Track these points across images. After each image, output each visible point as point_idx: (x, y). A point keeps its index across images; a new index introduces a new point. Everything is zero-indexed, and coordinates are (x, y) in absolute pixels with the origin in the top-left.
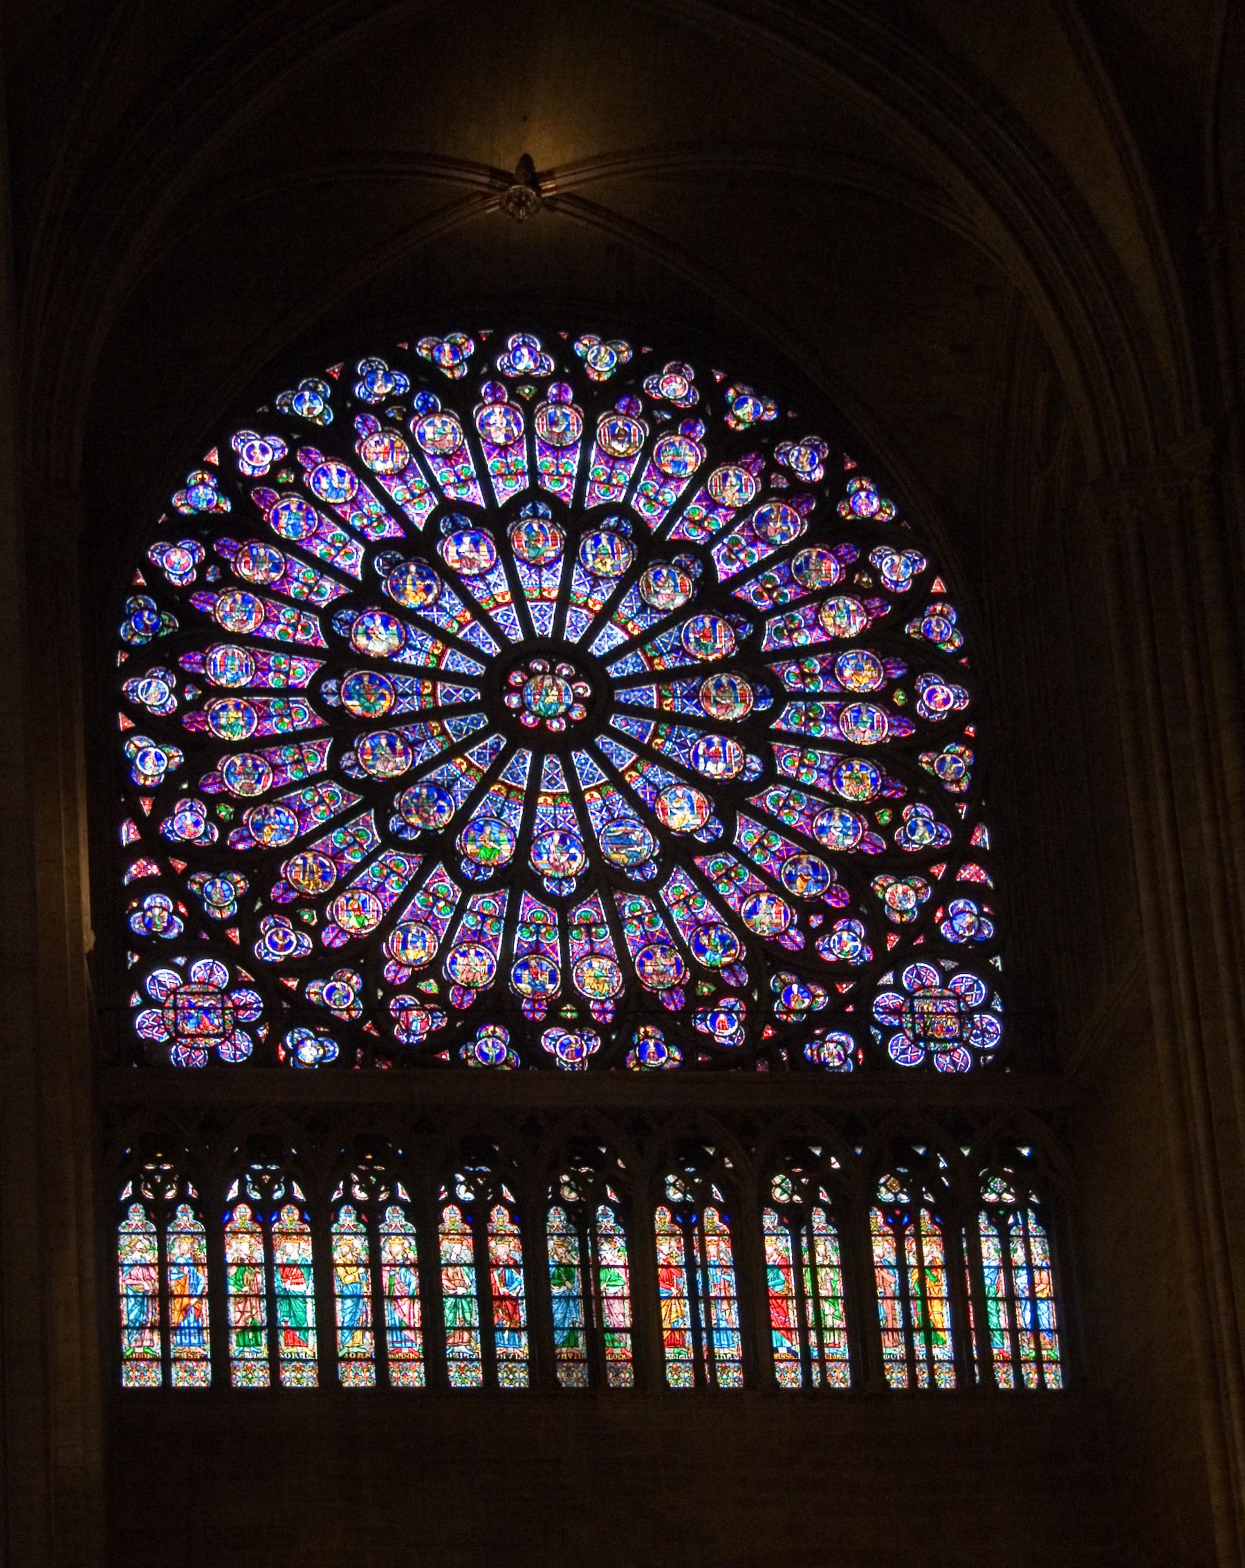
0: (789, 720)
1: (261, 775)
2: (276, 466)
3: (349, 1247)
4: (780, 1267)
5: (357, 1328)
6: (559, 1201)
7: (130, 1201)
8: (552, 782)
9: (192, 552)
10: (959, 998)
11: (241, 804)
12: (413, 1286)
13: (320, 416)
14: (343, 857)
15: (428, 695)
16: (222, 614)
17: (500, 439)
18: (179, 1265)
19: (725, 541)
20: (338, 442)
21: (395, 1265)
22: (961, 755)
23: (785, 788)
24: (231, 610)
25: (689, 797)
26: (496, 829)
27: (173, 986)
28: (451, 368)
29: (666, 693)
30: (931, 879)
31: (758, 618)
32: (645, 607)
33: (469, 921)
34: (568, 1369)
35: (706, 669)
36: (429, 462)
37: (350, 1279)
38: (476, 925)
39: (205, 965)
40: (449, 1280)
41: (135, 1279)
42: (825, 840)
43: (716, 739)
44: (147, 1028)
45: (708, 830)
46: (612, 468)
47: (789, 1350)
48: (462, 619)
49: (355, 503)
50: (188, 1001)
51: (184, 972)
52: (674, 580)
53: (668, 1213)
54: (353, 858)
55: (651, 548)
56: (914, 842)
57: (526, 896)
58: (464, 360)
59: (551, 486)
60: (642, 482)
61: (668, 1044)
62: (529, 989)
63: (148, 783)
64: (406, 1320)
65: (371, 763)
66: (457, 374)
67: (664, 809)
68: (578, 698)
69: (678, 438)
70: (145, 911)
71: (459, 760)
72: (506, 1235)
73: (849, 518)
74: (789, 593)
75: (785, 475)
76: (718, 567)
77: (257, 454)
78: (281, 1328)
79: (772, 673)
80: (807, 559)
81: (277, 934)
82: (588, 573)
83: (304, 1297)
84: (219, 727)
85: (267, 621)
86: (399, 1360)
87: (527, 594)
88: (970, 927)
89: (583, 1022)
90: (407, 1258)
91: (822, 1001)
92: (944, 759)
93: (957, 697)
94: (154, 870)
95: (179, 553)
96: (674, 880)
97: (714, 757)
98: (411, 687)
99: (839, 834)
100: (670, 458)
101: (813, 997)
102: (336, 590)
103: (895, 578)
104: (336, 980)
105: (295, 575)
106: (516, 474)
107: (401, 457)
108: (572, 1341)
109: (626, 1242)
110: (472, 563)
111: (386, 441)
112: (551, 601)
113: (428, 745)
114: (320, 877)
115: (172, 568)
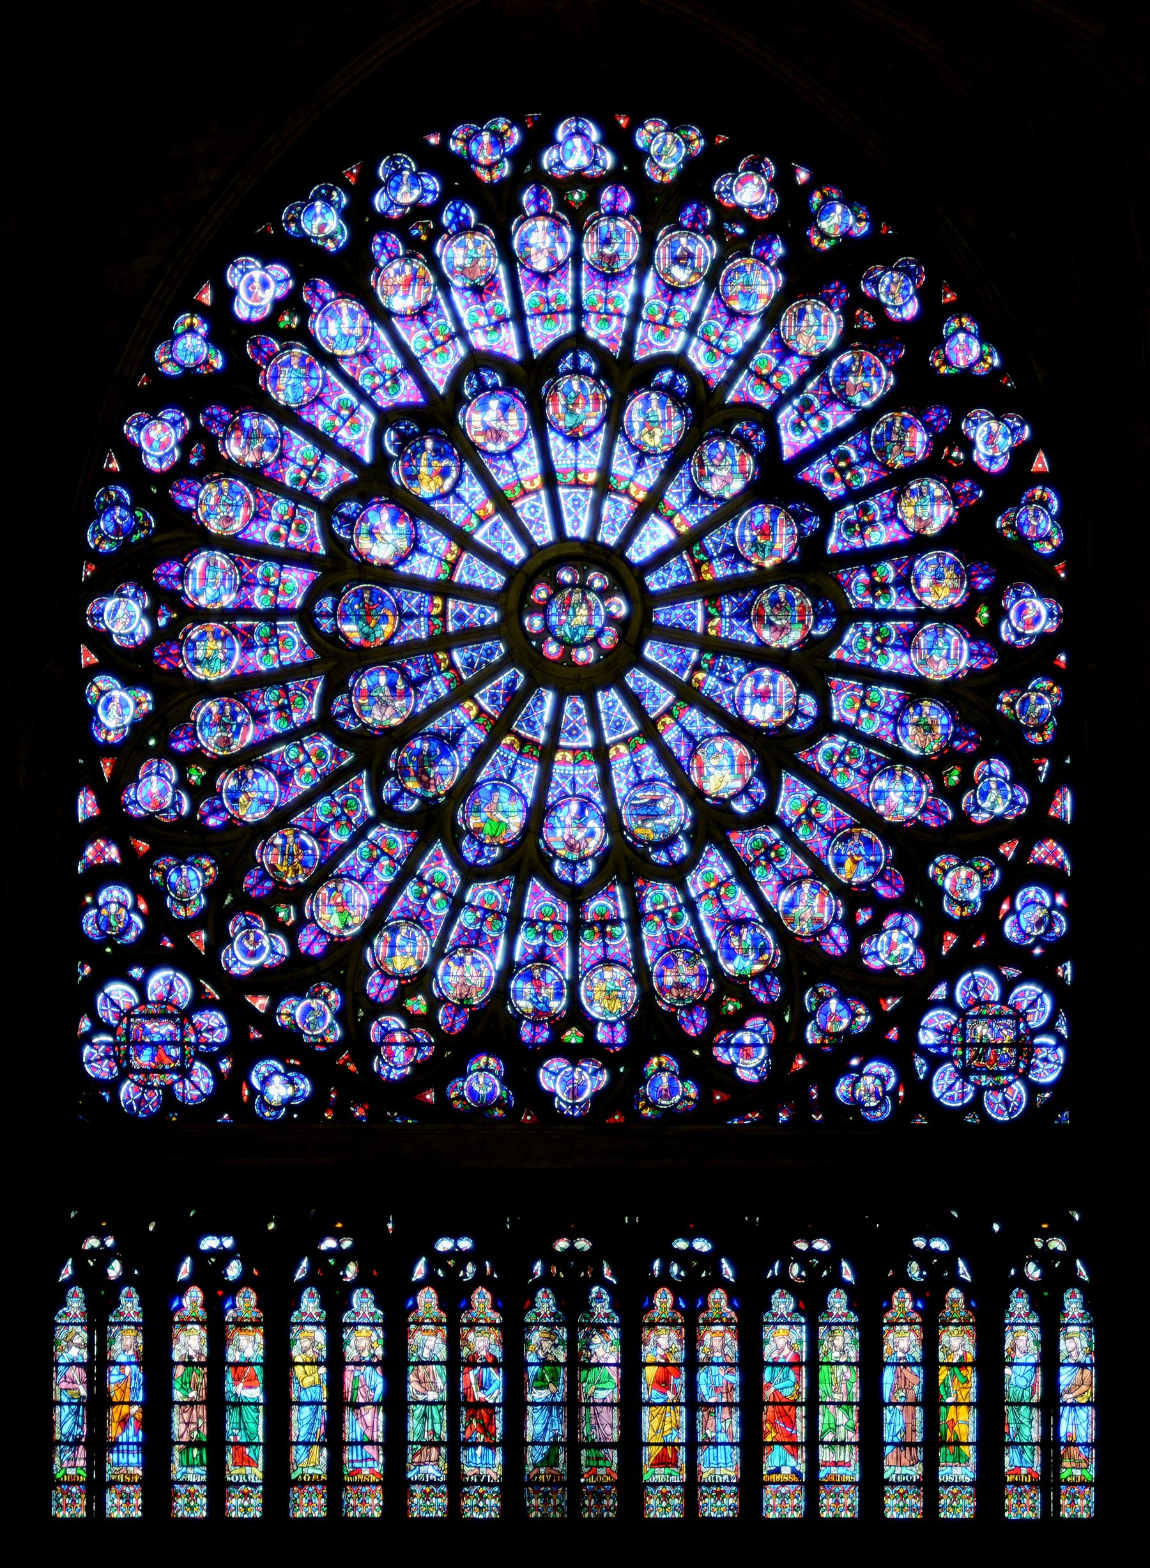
0: (854, 645)
1: (239, 726)
2: (279, 306)
3: (309, 1341)
4: (790, 1365)
5: (313, 1444)
6: (546, 1281)
7: (69, 1283)
8: (574, 733)
9: (174, 424)
10: (1019, 1016)
11: (216, 766)
12: (380, 1389)
13: (331, 237)
14: (327, 835)
15: (437, 616)
16: (205, 508)
17: (542, 265)
18: (120, 1364)
19: (796, 402)
20: (351, 273)
21: (358, 1364)
22: (1048, 693)
23: (841, 739)
24: (217, 504)
25: (730, 752)
26: (504, 795)
27: (127, 1006)
28: (490, 167)
29: (712, 611)
30: (1000, 861)
31: (827, 509)
32: (697, 494)
33: (466, 918)
34: (545, 1494)
35: (761, 580)
36: (455, 296)
37: (309, 1381)
38: (475, 923)
39: (165, 978)
40: (420, 1383)
41: (69, 1384)
42: (882, 809)
43: (767, 672)
44: (96, 1061)
45: (749, 795)
46: (671, 303)
47: (793, 1468)
48: (481, 513)
49: (366, 356)
50: (143, 1025)
51: (140, 986)
52: (733, 457)
53: (669, 1296)
54: (338, 836)
55: (707, 413)
56: (983, 810)
57: (535, 883)
58: (505, 155)
59: (595, 330)
60: (704, 321)
61: (683, 1079)
62: (530, 1006)
63: (110, 738)
64: (368, 1433)
65: (366, 708)
66: (496, 174)
67: (700, 767)
68: (611, 619)
69: (750, 261)
70: (100, 908)
71: (468, 704)
72: (486, 1324)
73: (943, 370)
74: (865, 476)
75: (871, 313)
76: (784, 440)
77: (256, 288)
78: (231, 1443)
79: (837, 582)
80: (890, 426)
81: (247, 936)
82: (633, 448)
83: (256, 1404)
84: (196, 662)
85: (257, 517)
86: (359, 1483)
87: (560, 477)
88: (1039, 923)
89: (589, 1050)
90: (374, 1356)
91: (864, 1020)
92: (1028, 698)
93: (1050, 614)
94: (113, 853)
95: (159, 427)
96: (706, 861)
97: (764, 696)
98: (418, 606)
99: (899, 798)
100: (739, 288)
101: (854, 1015)
102: (337, 477)
103: (990, 453)
104: (312, 997)
105: (291, 454)
106: (557, 312)
107: (424, 290)
108: (552, 1460)
109: (622, 1334)
110: (498, 435)
111: (408, 268)
112: (586, 486)
113: (433, 685)
114: (300, 862)
115: (150, 446)
